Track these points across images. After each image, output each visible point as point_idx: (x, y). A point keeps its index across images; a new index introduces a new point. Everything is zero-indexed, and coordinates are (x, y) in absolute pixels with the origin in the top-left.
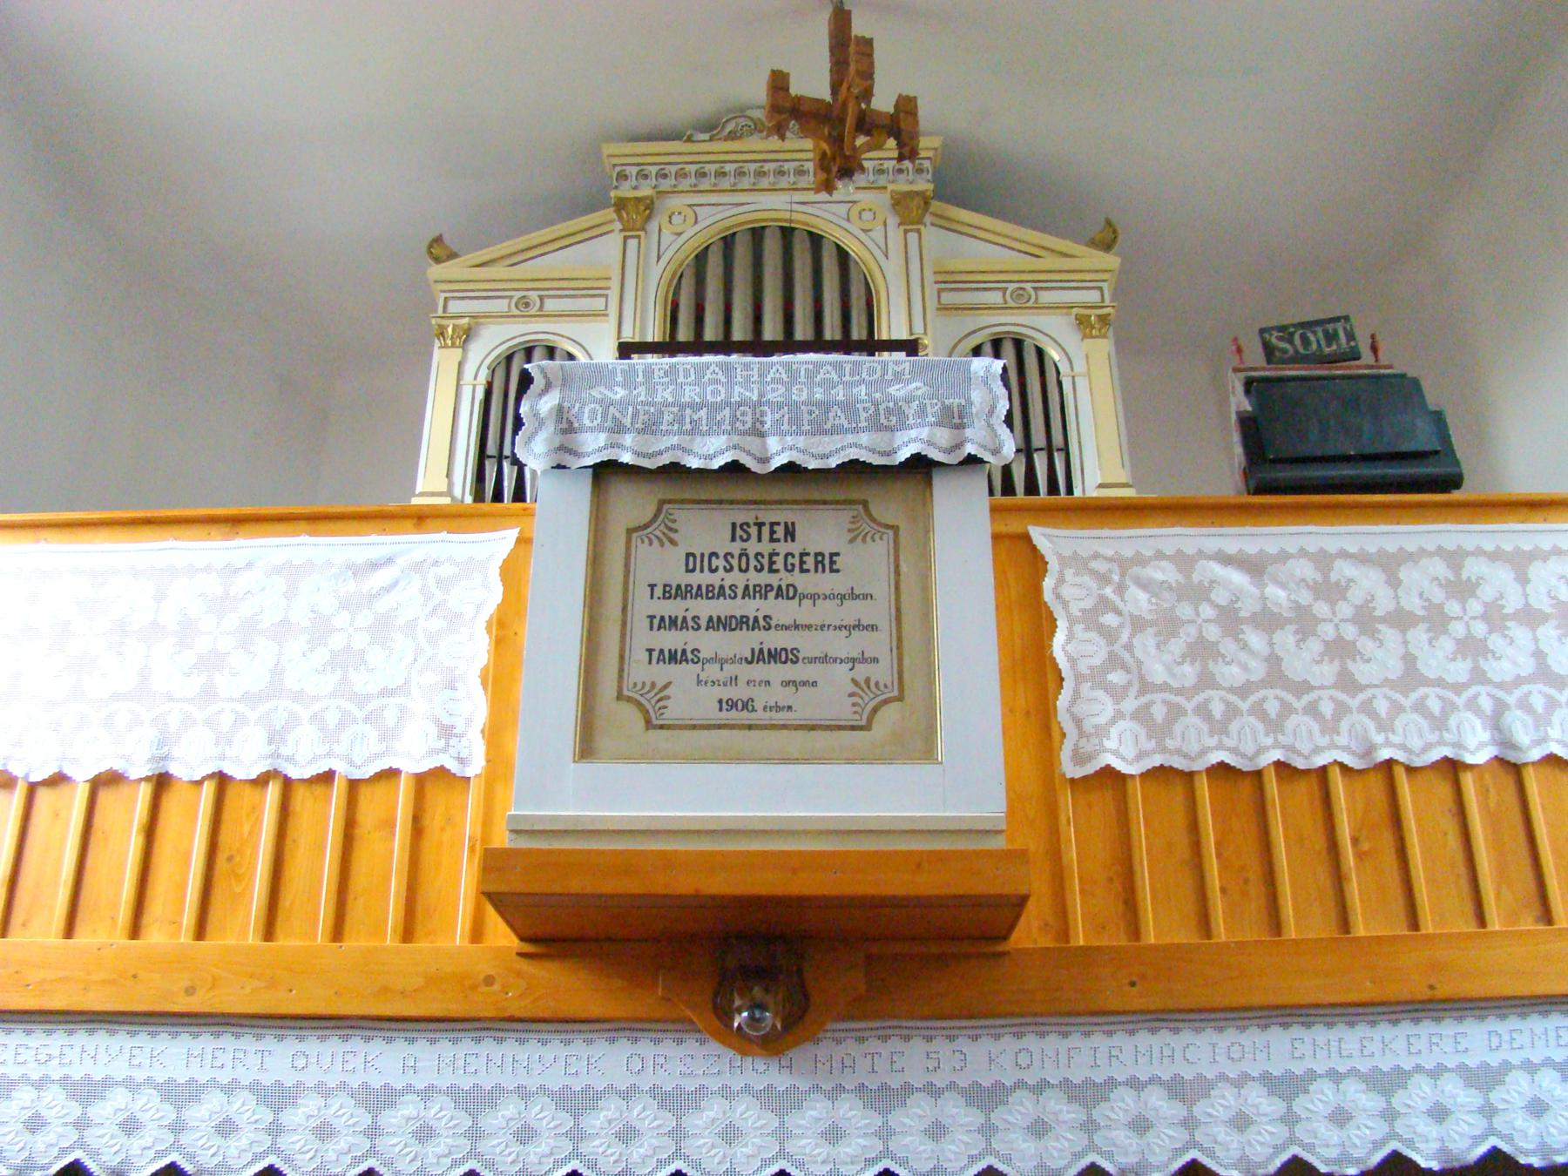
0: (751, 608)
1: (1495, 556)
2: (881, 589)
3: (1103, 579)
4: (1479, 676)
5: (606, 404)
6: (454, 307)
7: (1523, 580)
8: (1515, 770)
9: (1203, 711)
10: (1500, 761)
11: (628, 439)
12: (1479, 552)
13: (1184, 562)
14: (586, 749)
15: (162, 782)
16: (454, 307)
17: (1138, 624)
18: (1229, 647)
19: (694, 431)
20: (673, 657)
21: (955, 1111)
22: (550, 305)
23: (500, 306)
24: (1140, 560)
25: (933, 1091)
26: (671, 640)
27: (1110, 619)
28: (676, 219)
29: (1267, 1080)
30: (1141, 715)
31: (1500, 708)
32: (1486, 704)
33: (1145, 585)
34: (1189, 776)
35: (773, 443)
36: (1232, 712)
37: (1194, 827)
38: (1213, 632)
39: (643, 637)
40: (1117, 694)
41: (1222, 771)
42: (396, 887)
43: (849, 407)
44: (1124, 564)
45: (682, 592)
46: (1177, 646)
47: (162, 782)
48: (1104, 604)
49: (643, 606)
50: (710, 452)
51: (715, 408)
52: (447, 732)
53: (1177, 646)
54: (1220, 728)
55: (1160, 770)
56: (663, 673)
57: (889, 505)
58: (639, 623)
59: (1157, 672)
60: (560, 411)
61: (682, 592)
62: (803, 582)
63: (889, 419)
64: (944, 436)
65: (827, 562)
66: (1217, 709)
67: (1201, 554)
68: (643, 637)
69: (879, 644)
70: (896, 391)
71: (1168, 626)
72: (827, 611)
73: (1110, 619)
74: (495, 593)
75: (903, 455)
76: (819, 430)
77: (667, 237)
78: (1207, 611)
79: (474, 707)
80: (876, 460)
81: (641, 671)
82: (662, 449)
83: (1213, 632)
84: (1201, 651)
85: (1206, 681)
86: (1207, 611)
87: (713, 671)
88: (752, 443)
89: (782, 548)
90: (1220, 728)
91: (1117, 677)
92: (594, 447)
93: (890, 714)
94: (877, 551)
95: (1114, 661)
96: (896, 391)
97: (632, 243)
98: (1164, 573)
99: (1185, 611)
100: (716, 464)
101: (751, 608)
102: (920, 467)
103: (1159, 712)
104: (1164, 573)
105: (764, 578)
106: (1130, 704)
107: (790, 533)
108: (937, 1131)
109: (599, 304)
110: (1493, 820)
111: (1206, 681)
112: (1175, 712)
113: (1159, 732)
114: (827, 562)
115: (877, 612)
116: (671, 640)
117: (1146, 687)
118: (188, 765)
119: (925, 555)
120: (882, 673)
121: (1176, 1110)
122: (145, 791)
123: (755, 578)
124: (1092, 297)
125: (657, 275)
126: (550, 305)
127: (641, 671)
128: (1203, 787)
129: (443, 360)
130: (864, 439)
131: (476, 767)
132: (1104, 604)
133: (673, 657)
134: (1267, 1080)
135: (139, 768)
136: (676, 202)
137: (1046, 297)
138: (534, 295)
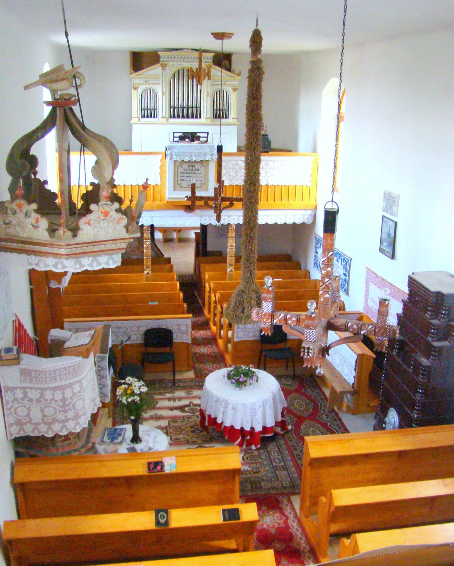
0: (191, 175)
1: (272, 161)
2: (203, 173)
3: (227, 163)
4: (266, 175)
5: (175, 152)
6: (135, 82)
7: (274, 163)
8: (268, 186)
9: (236, 178)
10: (267, 185)
11: (178, 157)
12: (270, 160)
13: (236, 161)
14: (175, 189)
15: (124, 185)
16: (135, 82)
17: (230, 168)
18: (240, 171)
19: (185, 156)
20: (183, 180)
21: (208, 218)
22: (150, 82)
23: (142, 82)
24: (232, 161)
25: (205, 216)
26: (182, 178)
27: (227, 168)
28: (171, 67)
29: (237, 216)
30: (229, 179)
31: (268, 179)
32: (266, 179)
33: (232, 164)
34: (233, 186)
35: (193, 158)
36: (239, 179)
37: (233, 190)
38: (238, 169)
39: (180, 178)
40: (227, 176)
41: (237, 185)
42: (152, 197)
43: (201, 153)
44: (230, 161)
45: (183, 173)
46: (234, 171)
47: (124, 185)
48: (227, 166)
49: (180, 175)
50: (187, 159)
51: (187, 153)
52: (156, 180)
53: (234, 171)
54: (237, 181)
55: (231, 185)
56: (183, 182)
57: (205, 164)
58: (179, 177)
59: (232, 174)
60: (170, 153)
61: (183, 173)
62: (196, 172)
63: (205, 155)
64: (211, 157)
65: (198, 170)
66: (237, 178)
67: (238, 160)
68: (180, 178)
69: (203, 179)
70: (206, 151)
71: (233, 168)
72: (198, 175)
73: (227, 168)
74: (159, 164)
75: (207, 159)
76: (198, 156)
77: (169, 71)
78: (238, 167)
79: (159, 177)
80: (204, 160)
81: (180, 182)
82: (182, 158)
83: (238, 169)
84: (237, 172)
85: (237, 175)
86: (238, 167)
87: (186, 182)
88: (191, 158)
89: (194, 168)
90: (237, 181)
91: (227, 175)
92: (174, 158)
93: (204, 186)
94: (203, 168)
95: (227, 173)
96: (206, 151)
97: (164, 72)
98: (234, 162)
99: (235, 167)
100: (187, 160)
101: (191, 175)
102: (208, 160)
103: (231, 179)
104: (234, 162)
105: (192, 172)
106: (228, 178)
107: (194, 166)
108: (205, 220)
109: (158, 82)
110: (264, 191)
111: (237, 175)
112: (233, 179)
113: (231, 181)
114: (198, 170)
115: (203, 175)
116: (182, 178)
117: (230, 176)
118: (128, 184)
119: (208, 170)
120: (203, 182)
121: (228, 218)
122: (123, 187)
123: (192, 172)
124: (236, 83)
125: (168, 78)
126: (150, 82)
127: (180, 182)
128: (235, 187)
129: (133, 92)
130: (203, 157)
131: (159, 184)
132: (227, 166)
133: (183, 180)
134: (237, 216)
135: (122, 185)
136: (171, 63)
137: (229, 83)
138: (148, 80)
